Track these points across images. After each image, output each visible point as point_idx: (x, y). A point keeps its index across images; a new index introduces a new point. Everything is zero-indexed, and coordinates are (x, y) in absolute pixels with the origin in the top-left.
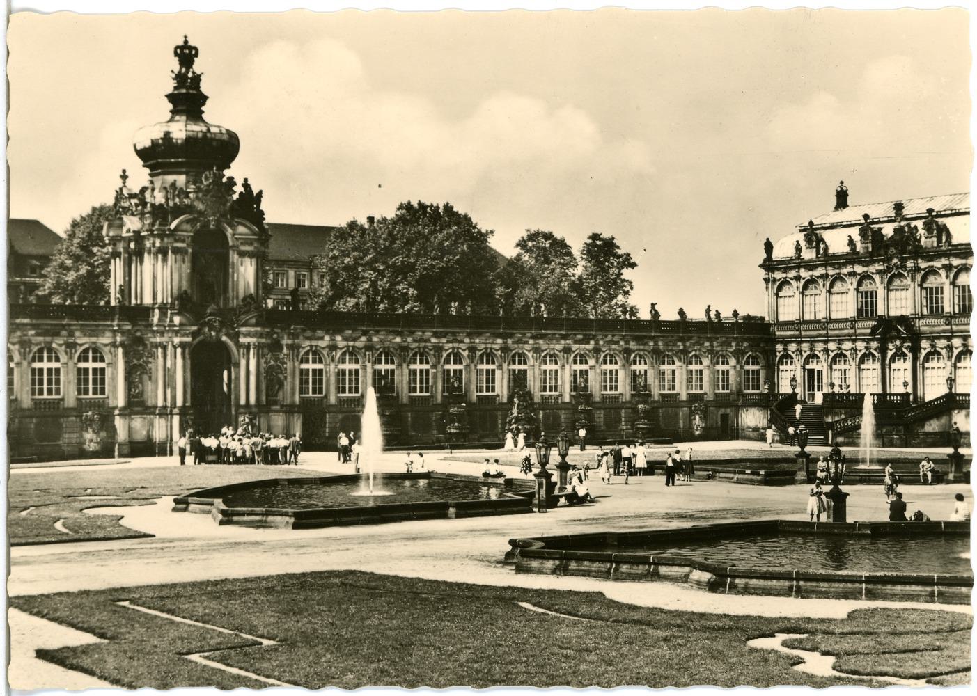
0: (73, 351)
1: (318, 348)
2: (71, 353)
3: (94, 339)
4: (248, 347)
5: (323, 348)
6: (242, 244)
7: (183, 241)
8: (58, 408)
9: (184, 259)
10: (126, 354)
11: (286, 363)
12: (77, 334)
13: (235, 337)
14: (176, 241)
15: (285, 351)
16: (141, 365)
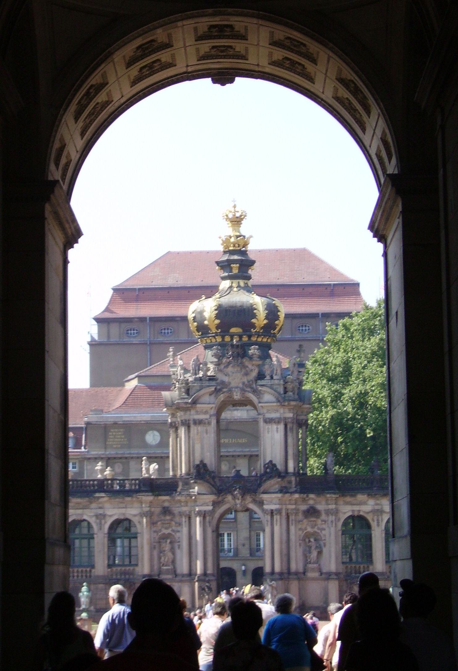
0: (103, 521)
1: (361, 513)
2: (101, 523)
3: (123, 511)
4: (272, 512)
5: (368, 513)
6: (268, 411)
7: (206, 413)
8: (90, 576)
9: (207, 430)
10: (152, 523)
11: (324, 529)
12: (107, 505)
13: (261, 503)
14: (197, 413)
15: (323, 517)
16: (169, 534)
